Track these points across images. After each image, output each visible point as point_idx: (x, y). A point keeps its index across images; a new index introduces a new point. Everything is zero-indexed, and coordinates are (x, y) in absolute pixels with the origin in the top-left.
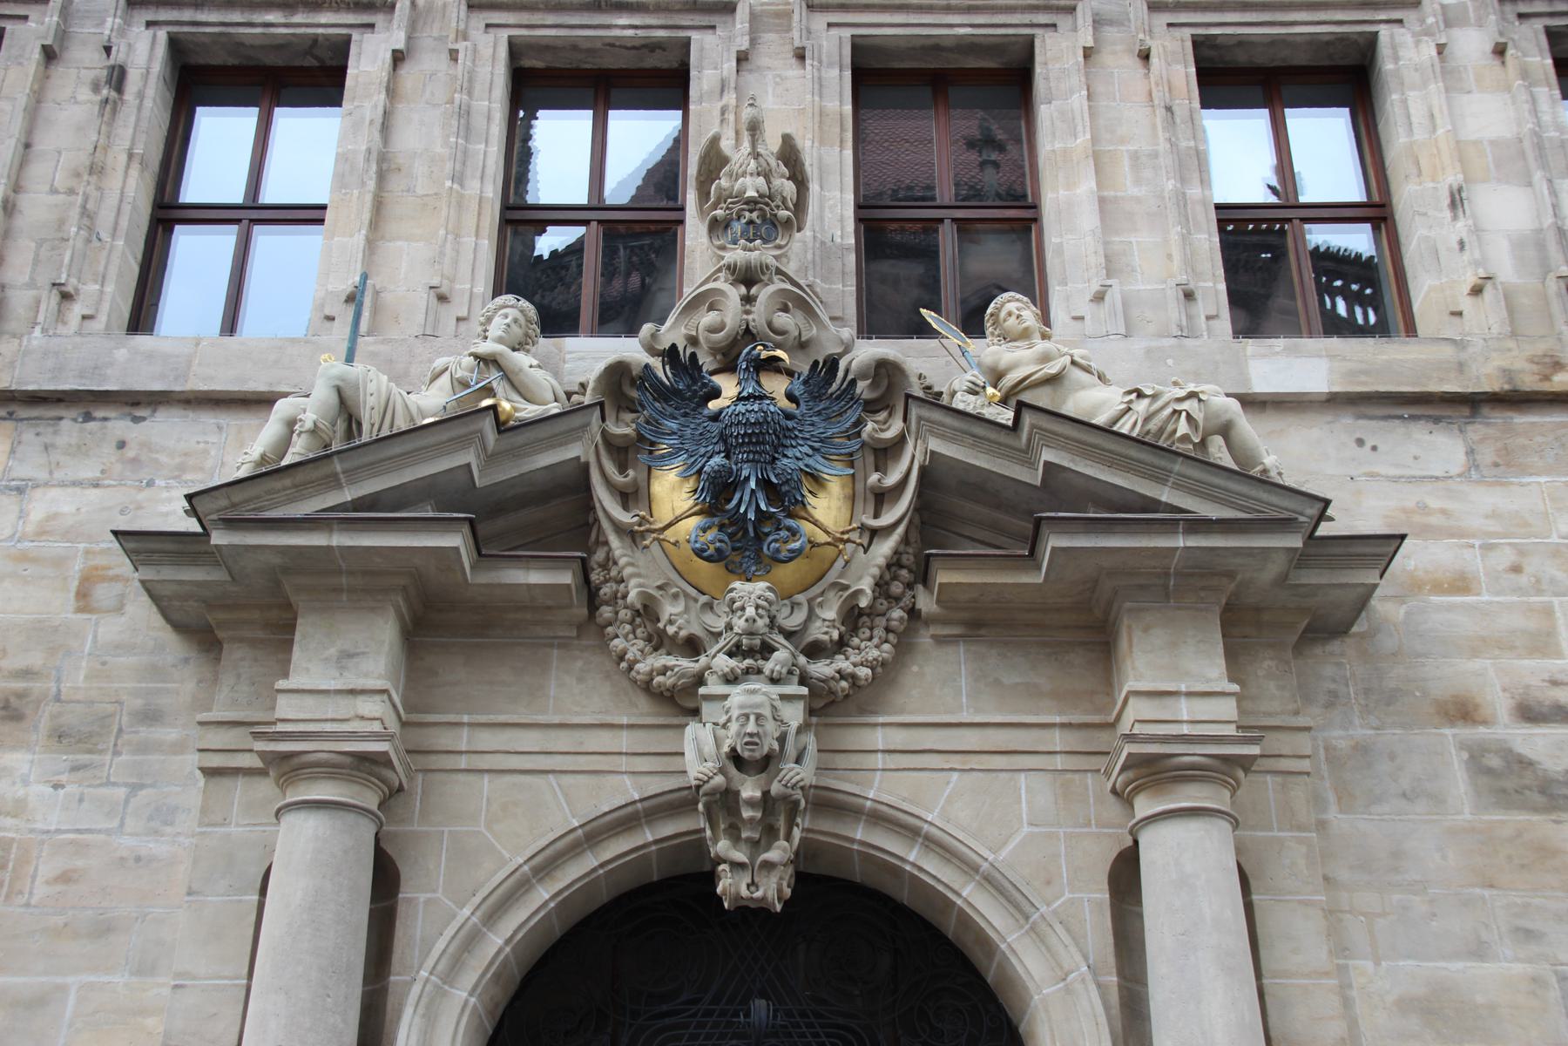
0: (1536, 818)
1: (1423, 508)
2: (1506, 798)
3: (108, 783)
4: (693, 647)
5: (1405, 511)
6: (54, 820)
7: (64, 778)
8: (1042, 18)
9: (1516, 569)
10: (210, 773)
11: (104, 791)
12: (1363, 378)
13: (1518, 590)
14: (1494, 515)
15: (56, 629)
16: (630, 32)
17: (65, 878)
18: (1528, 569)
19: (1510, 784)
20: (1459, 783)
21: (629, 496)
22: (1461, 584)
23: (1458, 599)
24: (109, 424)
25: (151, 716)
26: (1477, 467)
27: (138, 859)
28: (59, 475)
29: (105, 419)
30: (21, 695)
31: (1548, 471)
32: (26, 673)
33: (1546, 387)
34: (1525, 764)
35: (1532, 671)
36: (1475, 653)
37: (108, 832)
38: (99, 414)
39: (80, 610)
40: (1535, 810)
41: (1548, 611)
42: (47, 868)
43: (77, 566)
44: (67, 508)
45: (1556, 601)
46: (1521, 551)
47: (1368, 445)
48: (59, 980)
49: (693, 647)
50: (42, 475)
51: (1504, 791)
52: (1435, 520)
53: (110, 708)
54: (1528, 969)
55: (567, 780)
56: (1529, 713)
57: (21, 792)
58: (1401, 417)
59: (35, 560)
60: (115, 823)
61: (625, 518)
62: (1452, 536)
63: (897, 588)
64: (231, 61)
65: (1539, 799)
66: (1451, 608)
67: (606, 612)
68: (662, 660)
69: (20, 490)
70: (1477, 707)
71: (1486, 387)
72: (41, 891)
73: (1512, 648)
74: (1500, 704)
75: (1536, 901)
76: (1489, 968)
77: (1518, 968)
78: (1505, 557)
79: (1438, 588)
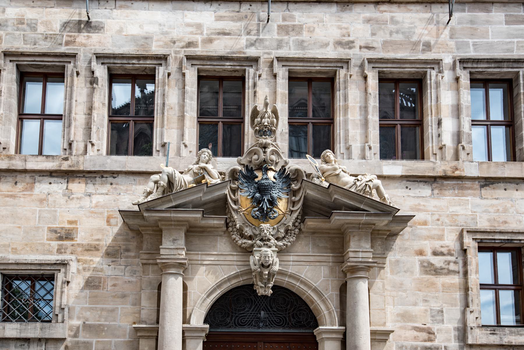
0: (432, 276)
1: (419, 204)
2: (426, 272)
3: (120, 265)
4: (250, 238)
5: (416, 205)
6: (110, 273)
7: (110, 264)
8: (339, 65)
9: (438, 220)
10: (143, 264)
11: (119, 267)
12: (410, 171)
13: (438, 225)
14: (435, 207)
15: (103, 230)
16: (230, 67)
17: (114, 285)
18: (441, 220)
19: (428, 269)
20: (417, 268)
21: (235, 202)
22: (425, 223)
23: (423, 227)
24: (108, 179)
25: (127, 250)
26: (433, 194)
27: (129, 282)
28: (98, 192)
29: (107, 177)
30: (98, 245)
31: (449, 196)
32: (98, 240)
33: (453, 175)
34: (432, 265)
35: (437, 244)
36: (425, 239)
37: (122, 276)
38: (105, 176)
39: (108, 225)
40: (432, 275)
41: (443, 230)
42: (110, 283)
43: (106, 214)
44: (101, 200)
45: (446, 227)
46: (440, 216)
47: (409, 188)
48: (116, 306)
49: (250, 238)
50: (94, 192)
51: (426, 271)
52: (421, 207)
53: (118, 248)
54: (425, 308)
55: (223, 266)
56: (435, 253)
57: (102, 267)
58: (417, 181)
59: (95, 213)
60: (123, 274)
61: (234, 206)
62: (425, 211)
63: (297, 224)
64: (123, 73)
65: (433, 272)
66: (421, 229)
67: (230, 229)
68: (245, 241)
69: (90, 196)
70: (424, 252)
71: (439, 174)
72: (109, 288)
73: (434, 239)
74: (429, 252)
75: (429, 294)
76: (417, 308)
77: (423, 308)
78: (436, 217)
79: (420, 224)
